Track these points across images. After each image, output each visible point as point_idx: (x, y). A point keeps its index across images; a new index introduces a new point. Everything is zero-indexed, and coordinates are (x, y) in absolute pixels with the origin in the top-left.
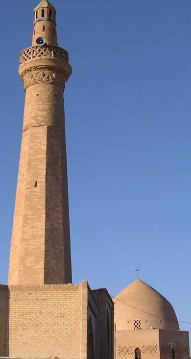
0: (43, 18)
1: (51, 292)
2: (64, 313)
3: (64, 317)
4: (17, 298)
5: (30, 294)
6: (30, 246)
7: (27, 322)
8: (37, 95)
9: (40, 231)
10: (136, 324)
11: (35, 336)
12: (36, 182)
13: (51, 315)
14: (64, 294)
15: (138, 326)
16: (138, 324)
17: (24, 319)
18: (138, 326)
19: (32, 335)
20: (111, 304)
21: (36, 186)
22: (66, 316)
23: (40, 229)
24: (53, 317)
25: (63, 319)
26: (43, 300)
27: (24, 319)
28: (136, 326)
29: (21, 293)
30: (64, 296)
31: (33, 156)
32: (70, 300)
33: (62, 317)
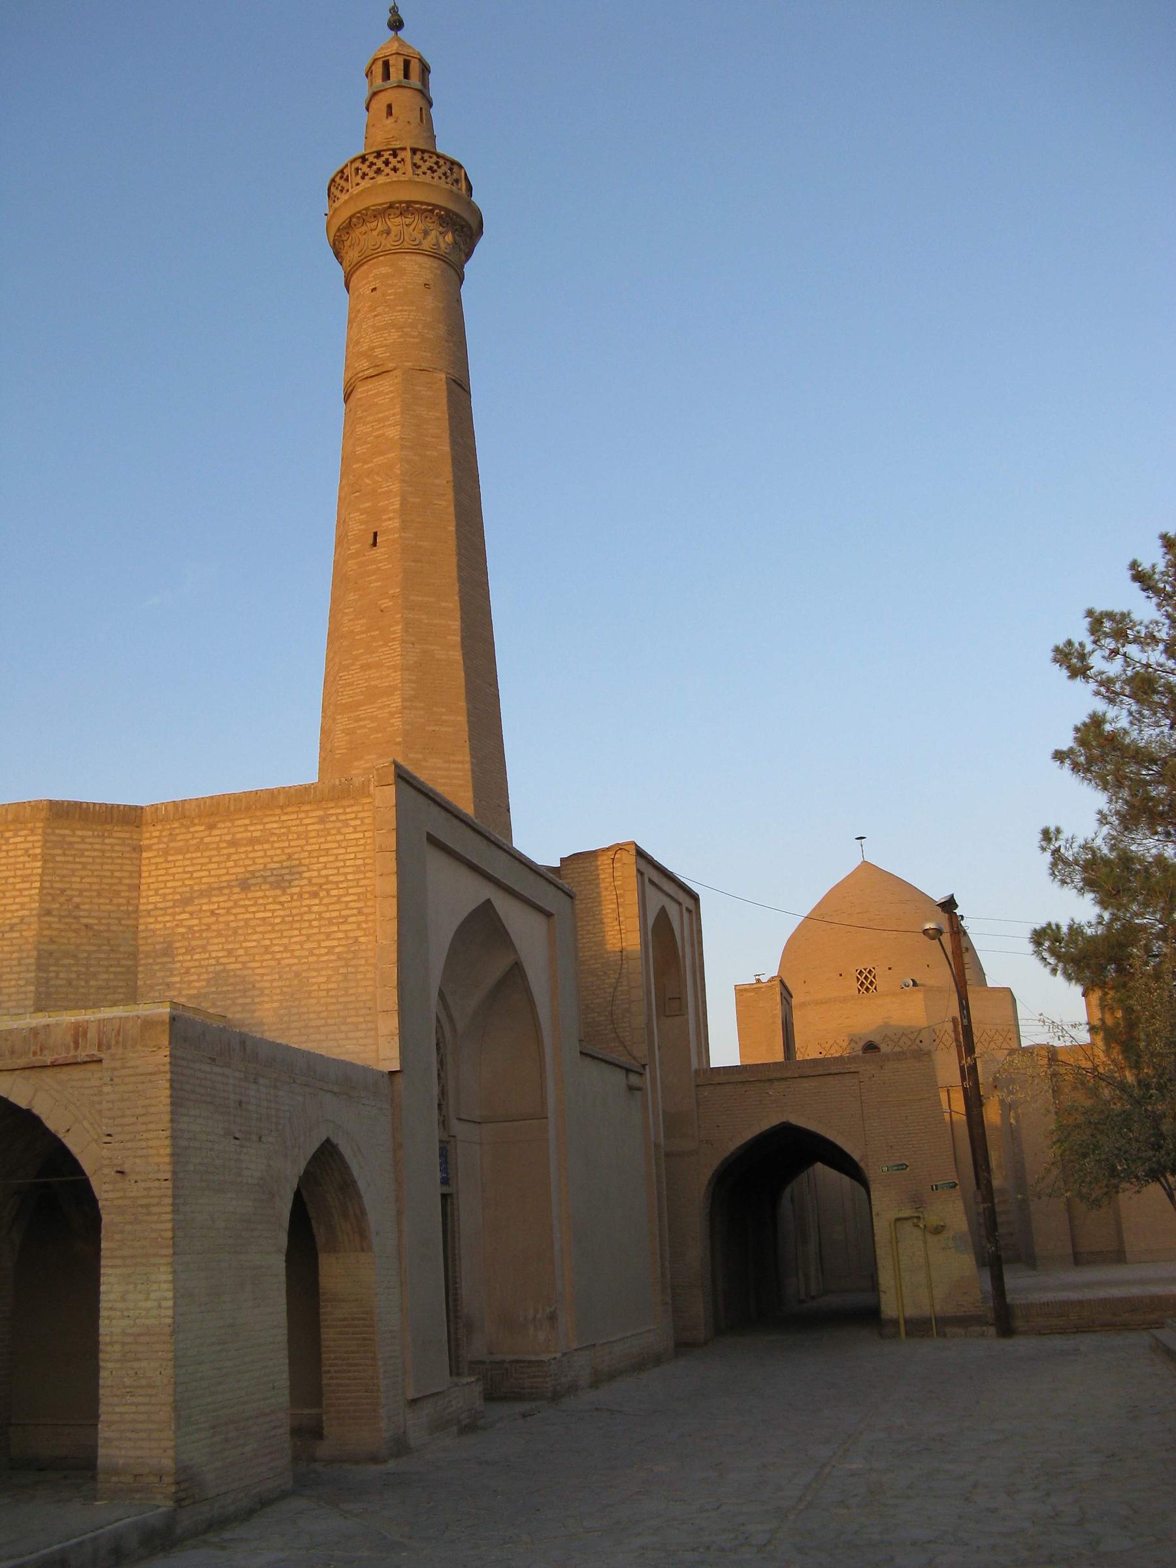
0: (388, 84)
1: (278, 811)
2: (322, 880)
3: (322, 894)
4: (172, 845)
5: (211, 827)
6: (361, 723)
7: (200, 924)
8: (374, 290)
9: (388, 676)
10: (862, 979)
11: (228, 971)
12: (375, 534)
13: (278, 892)
14: (320, 813)
15: (867, 984)
16: (866, 978)
17: (191, 914)
18: (867, 984)
19: (219, 968)
20: (687, 902)
21: (375, 544)
22: (328, 891)
23: (389, 668)
24: (283, 899)
25: (317, 901)
26: (252, 841)
27: (191, 914)
28: (862, 984)
29: (182, 825)
30: (322, 820)
31: (365, 462)
32: (339, 833)
33: (315, 895)
